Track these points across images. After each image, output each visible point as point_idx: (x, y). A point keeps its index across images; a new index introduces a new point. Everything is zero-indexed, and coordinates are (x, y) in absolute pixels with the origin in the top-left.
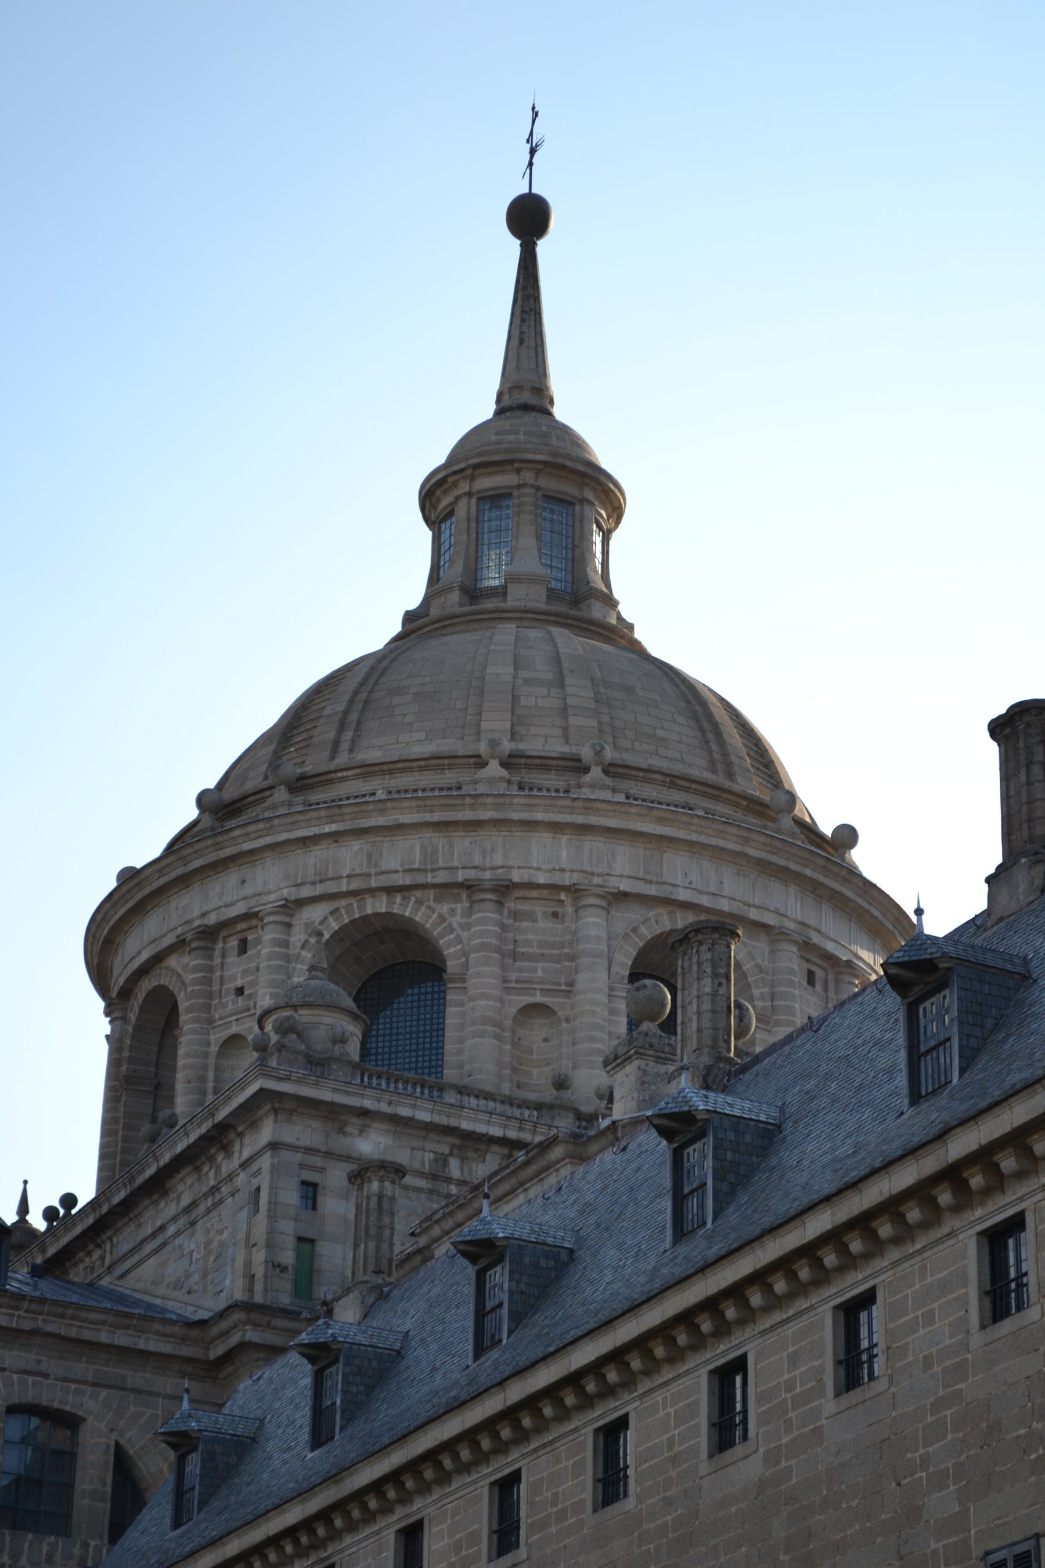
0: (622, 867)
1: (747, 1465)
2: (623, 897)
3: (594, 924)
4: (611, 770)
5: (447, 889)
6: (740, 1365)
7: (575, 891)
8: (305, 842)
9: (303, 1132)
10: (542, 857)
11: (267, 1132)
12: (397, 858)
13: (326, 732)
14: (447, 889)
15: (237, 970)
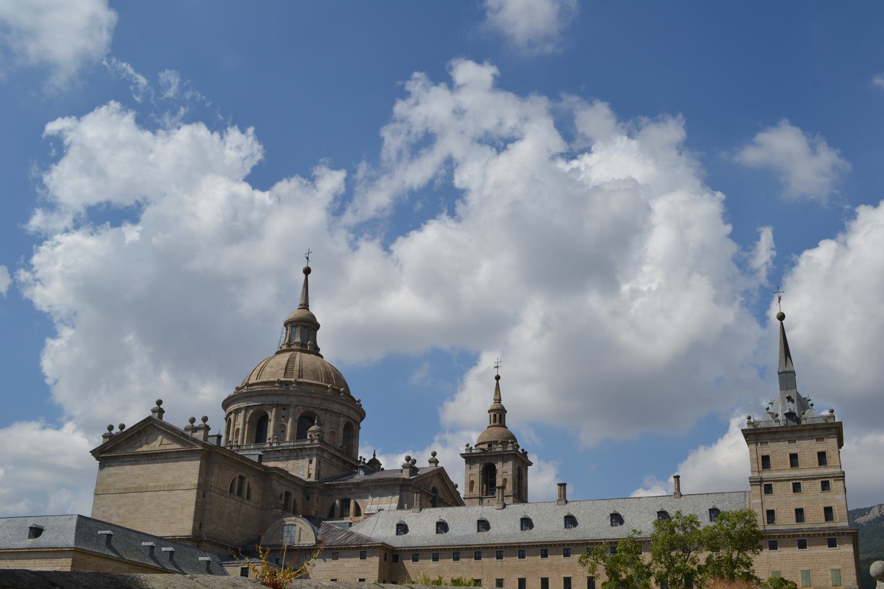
0: (345, 410)
1: (547, 561)
2: (345, 416)
3: (342, 419)
4: (345, 393)
5: (322, 409)
6: (546, 550)
7: (340, 414)
8: (301, 396)
9: (320, 453)
10: (336, 408)
11: (315, 452)
12: (316, 403)
13: (296, 373)
14: (322, 409)
15: (283, 413)
